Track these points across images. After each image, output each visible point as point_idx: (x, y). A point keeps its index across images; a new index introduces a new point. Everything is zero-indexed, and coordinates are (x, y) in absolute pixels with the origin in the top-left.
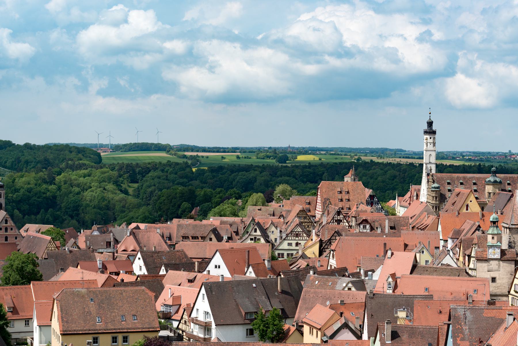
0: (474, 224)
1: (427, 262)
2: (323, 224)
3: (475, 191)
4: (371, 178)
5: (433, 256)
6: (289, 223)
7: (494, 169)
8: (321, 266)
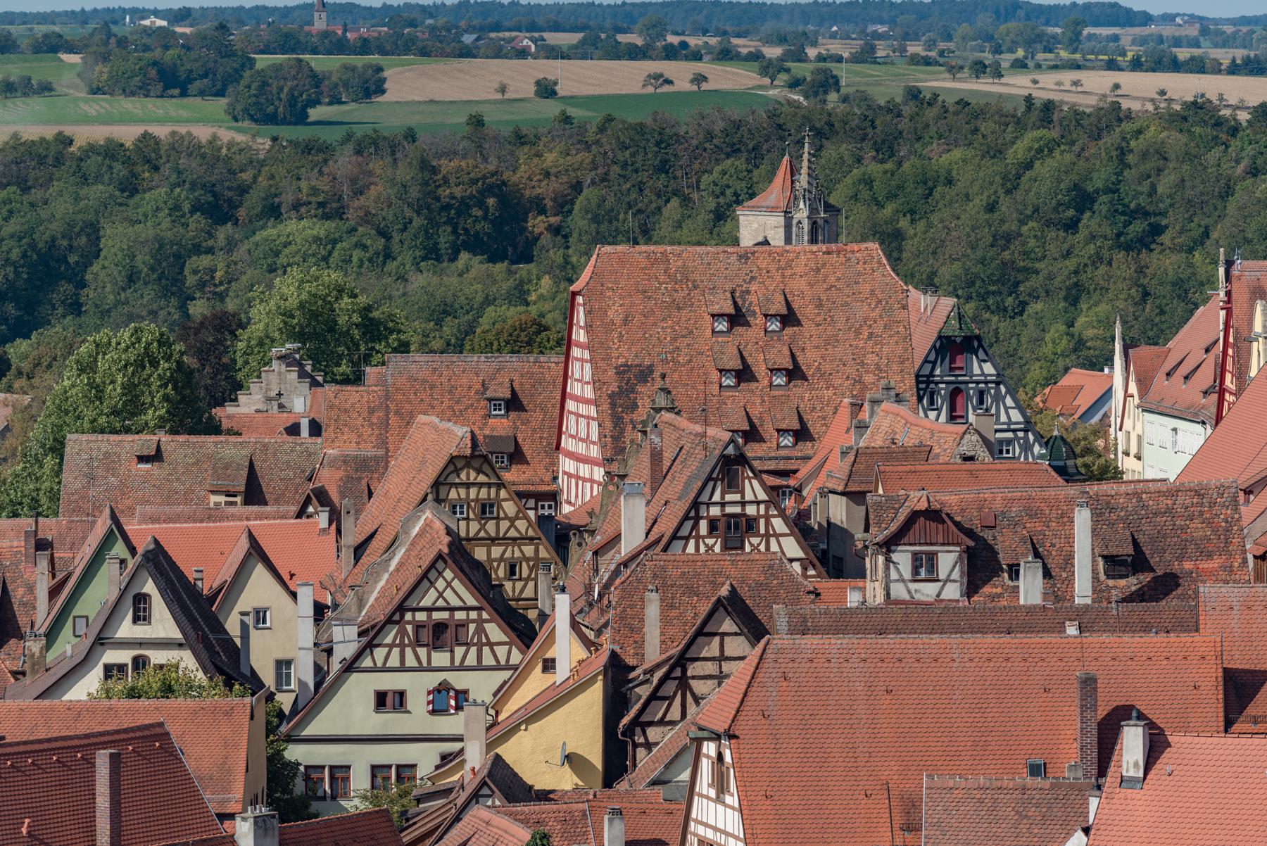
6: (377, 544)
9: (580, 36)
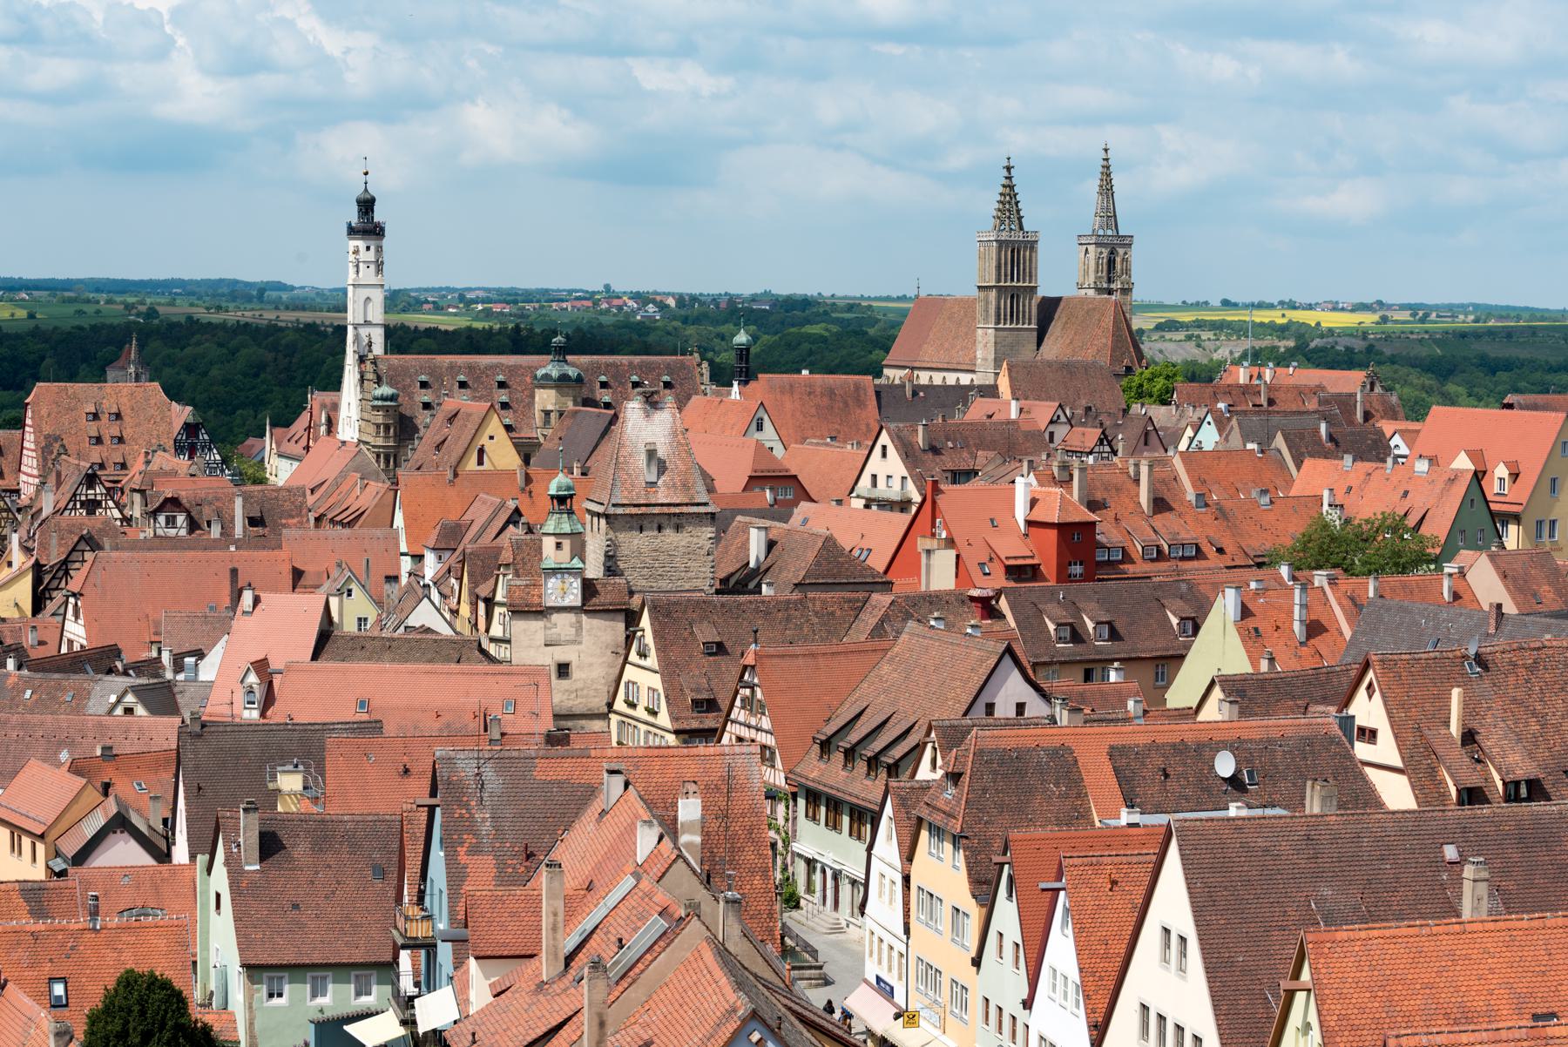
0: (503, 505)
1: (362, 621)
2: (44, 514)
3: (505, 406)
4: (190, 371)
5: (379, 603)
7: (558, 339)
8: (41, 643)
9: (46, 293)
